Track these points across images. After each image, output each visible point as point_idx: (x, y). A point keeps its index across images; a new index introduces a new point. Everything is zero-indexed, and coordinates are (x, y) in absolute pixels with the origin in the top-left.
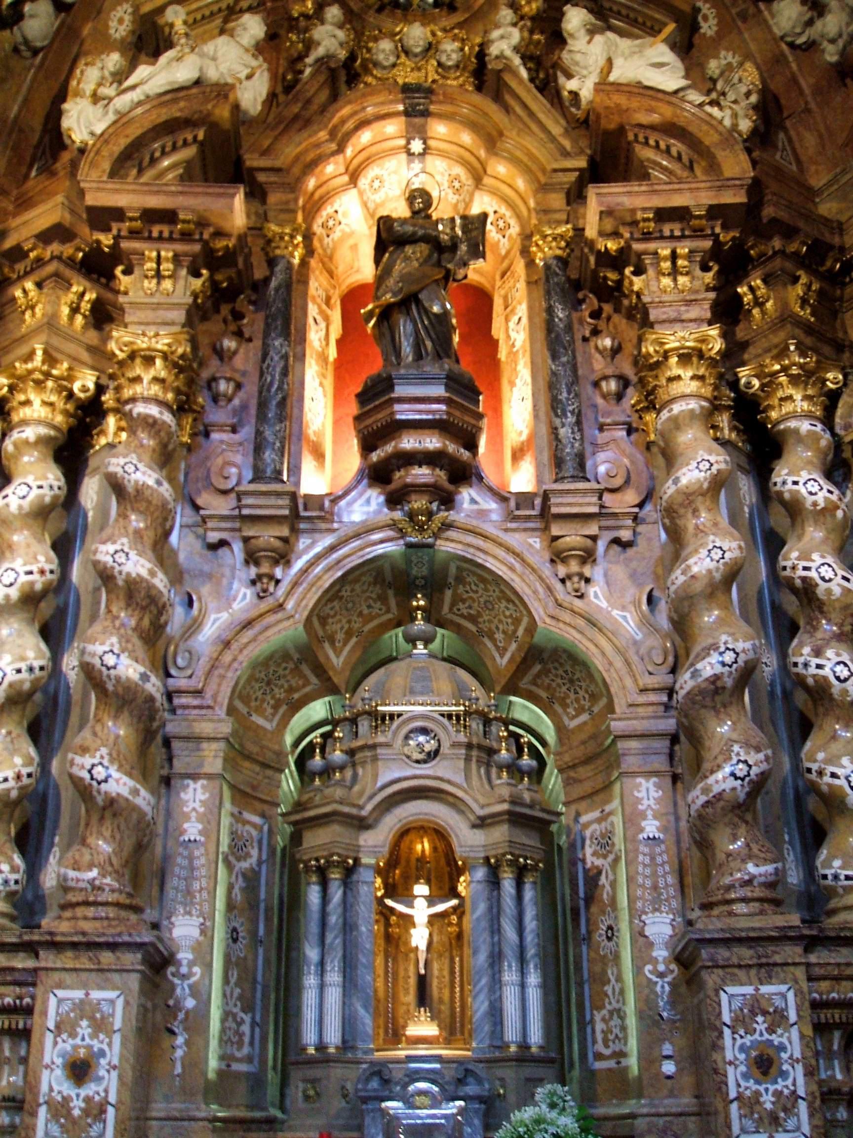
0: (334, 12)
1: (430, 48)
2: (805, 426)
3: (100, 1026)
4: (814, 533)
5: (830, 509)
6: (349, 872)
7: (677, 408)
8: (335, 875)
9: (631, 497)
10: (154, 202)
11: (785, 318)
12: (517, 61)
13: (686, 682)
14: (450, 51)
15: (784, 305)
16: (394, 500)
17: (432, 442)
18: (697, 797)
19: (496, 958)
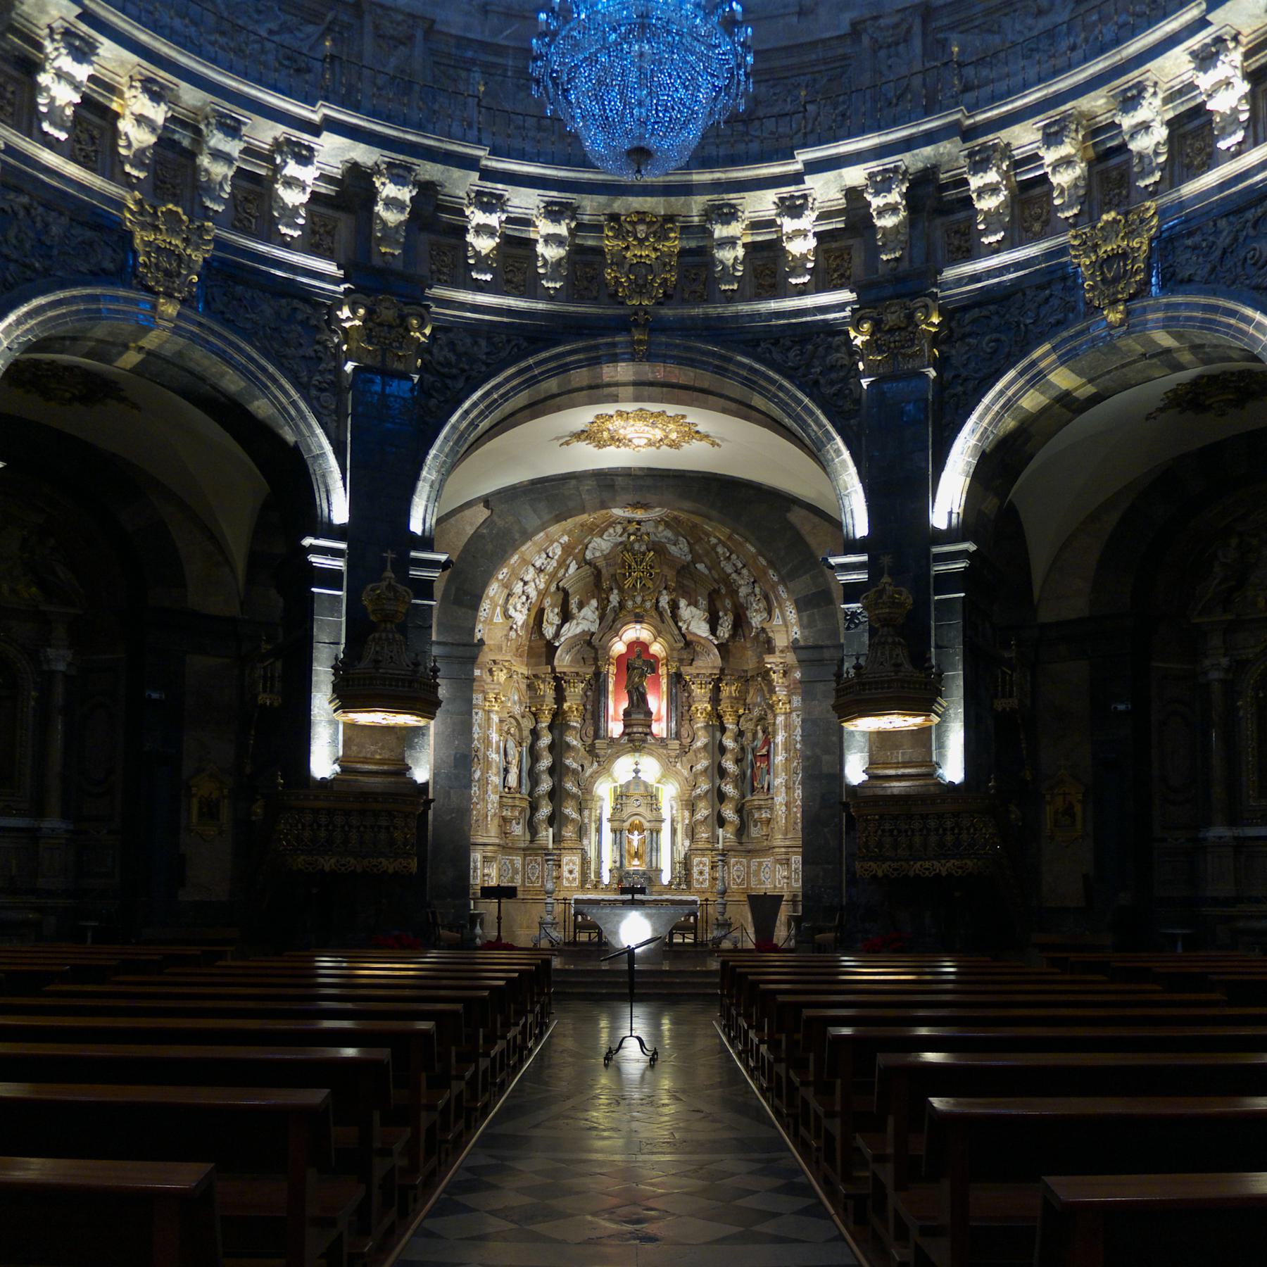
0: (616, 591)
1: (643, 601)
2: (731, 727)
3: (574, 864)
4: (729, 756)
5: (734, 749)
6: (621, 831)
7: (699, 725)
8: (618, 833)
9: (689, 740)
10: (573, 670)
11: (730, 697)
12: (667, 607)
13: (694, 794)
14: (648, 604)
15: (731, 692)
16: (630, 741)
17: (640, 730)
18: (694, 819)
19: (651, 850)
